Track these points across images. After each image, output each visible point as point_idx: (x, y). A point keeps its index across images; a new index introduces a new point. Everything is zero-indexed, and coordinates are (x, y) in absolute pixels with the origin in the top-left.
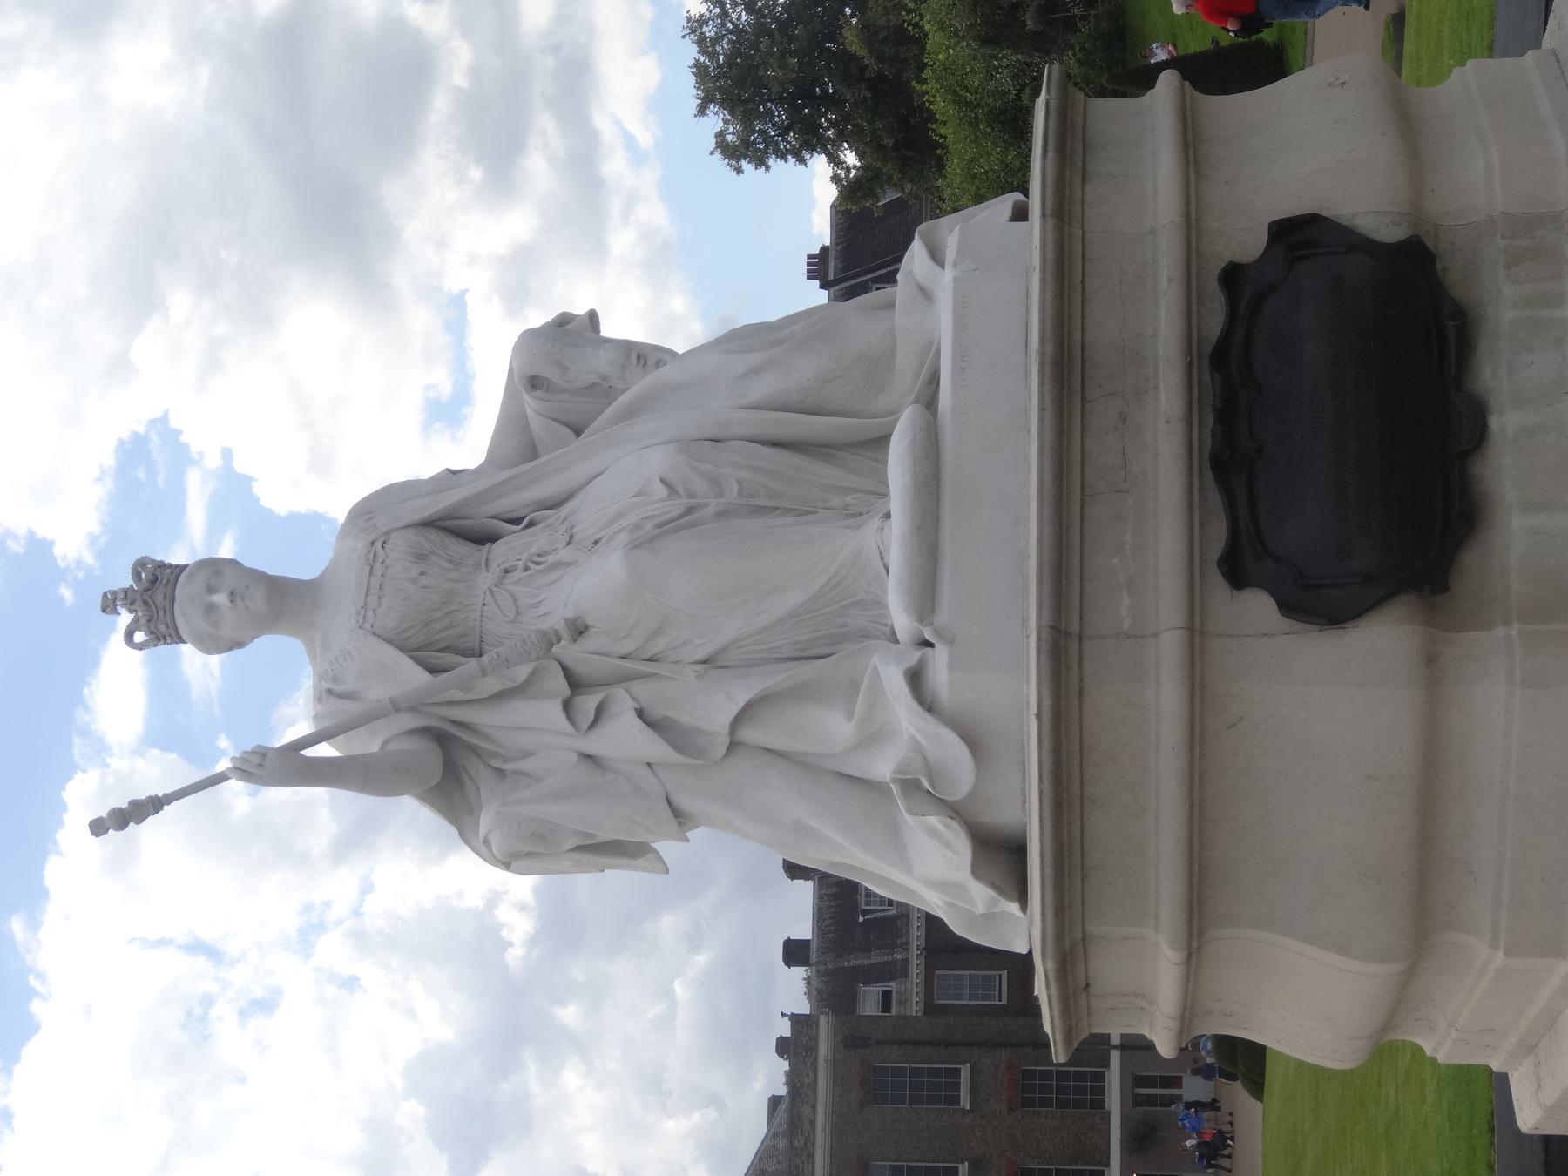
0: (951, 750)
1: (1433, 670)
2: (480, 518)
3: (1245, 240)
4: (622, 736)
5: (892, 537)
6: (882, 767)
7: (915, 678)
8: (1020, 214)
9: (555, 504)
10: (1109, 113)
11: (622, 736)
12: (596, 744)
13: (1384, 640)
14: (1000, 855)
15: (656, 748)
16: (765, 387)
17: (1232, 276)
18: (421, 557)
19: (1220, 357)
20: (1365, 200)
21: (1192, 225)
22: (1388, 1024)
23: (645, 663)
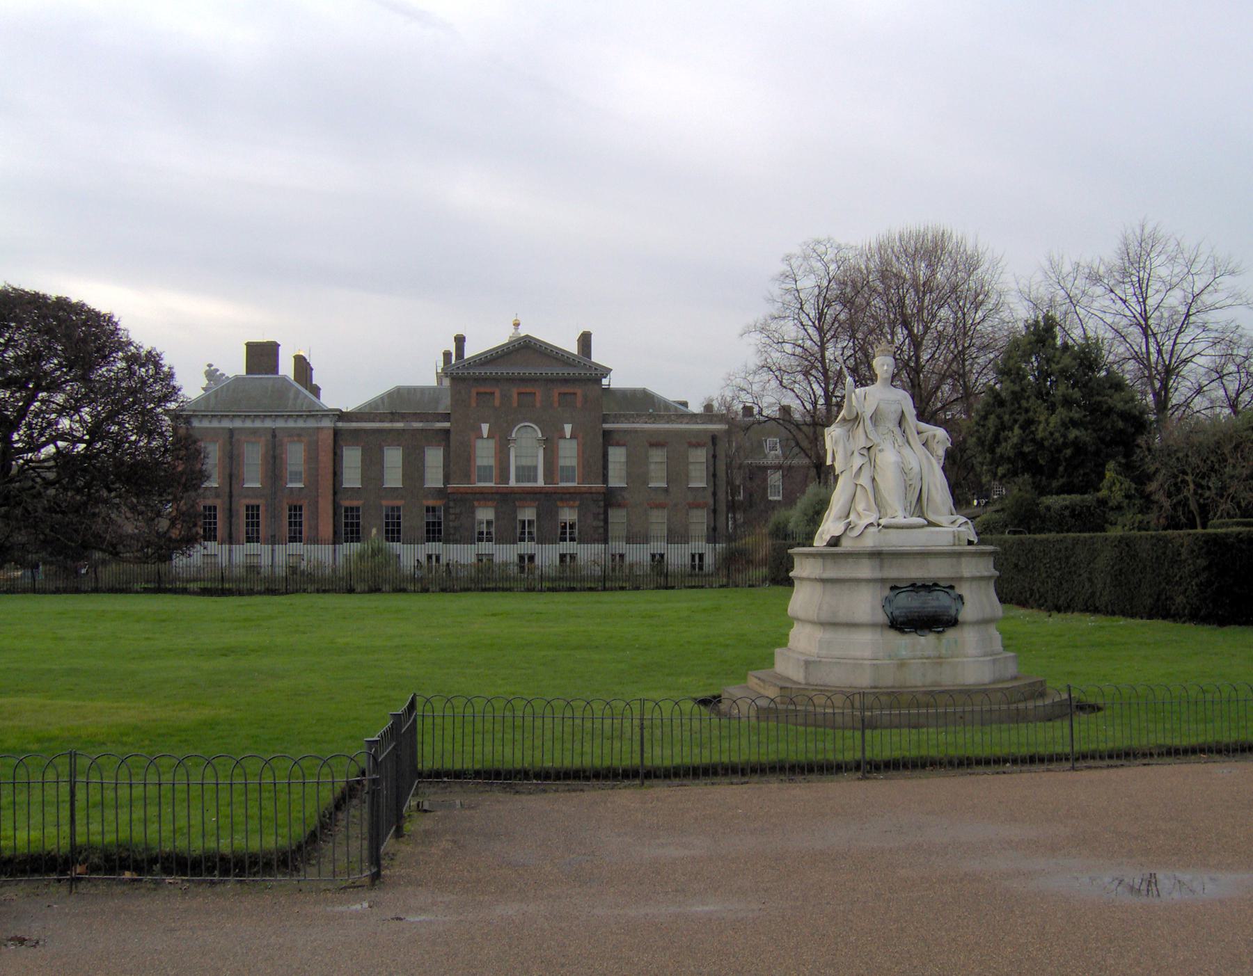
0: (856, 532)
1: (874, 625)
2: (904, 424)
3: (958, 591)
4: (857, 461)
5: (900, 520)
6: (852, 517)
7: (872, 524)
8: (970, 543)
9: (908, 442)
10: (990, 562)
11: (857, 461)
12: (856, 453)
13: (882, 618)
14: (835, 541)
15: (855, 469)
16: (933, 491)
17: (952, 587)
19: (936, 585)
20: (968, 612)
21: (961, 579)
22: (798, 619)
23: (873, 463)
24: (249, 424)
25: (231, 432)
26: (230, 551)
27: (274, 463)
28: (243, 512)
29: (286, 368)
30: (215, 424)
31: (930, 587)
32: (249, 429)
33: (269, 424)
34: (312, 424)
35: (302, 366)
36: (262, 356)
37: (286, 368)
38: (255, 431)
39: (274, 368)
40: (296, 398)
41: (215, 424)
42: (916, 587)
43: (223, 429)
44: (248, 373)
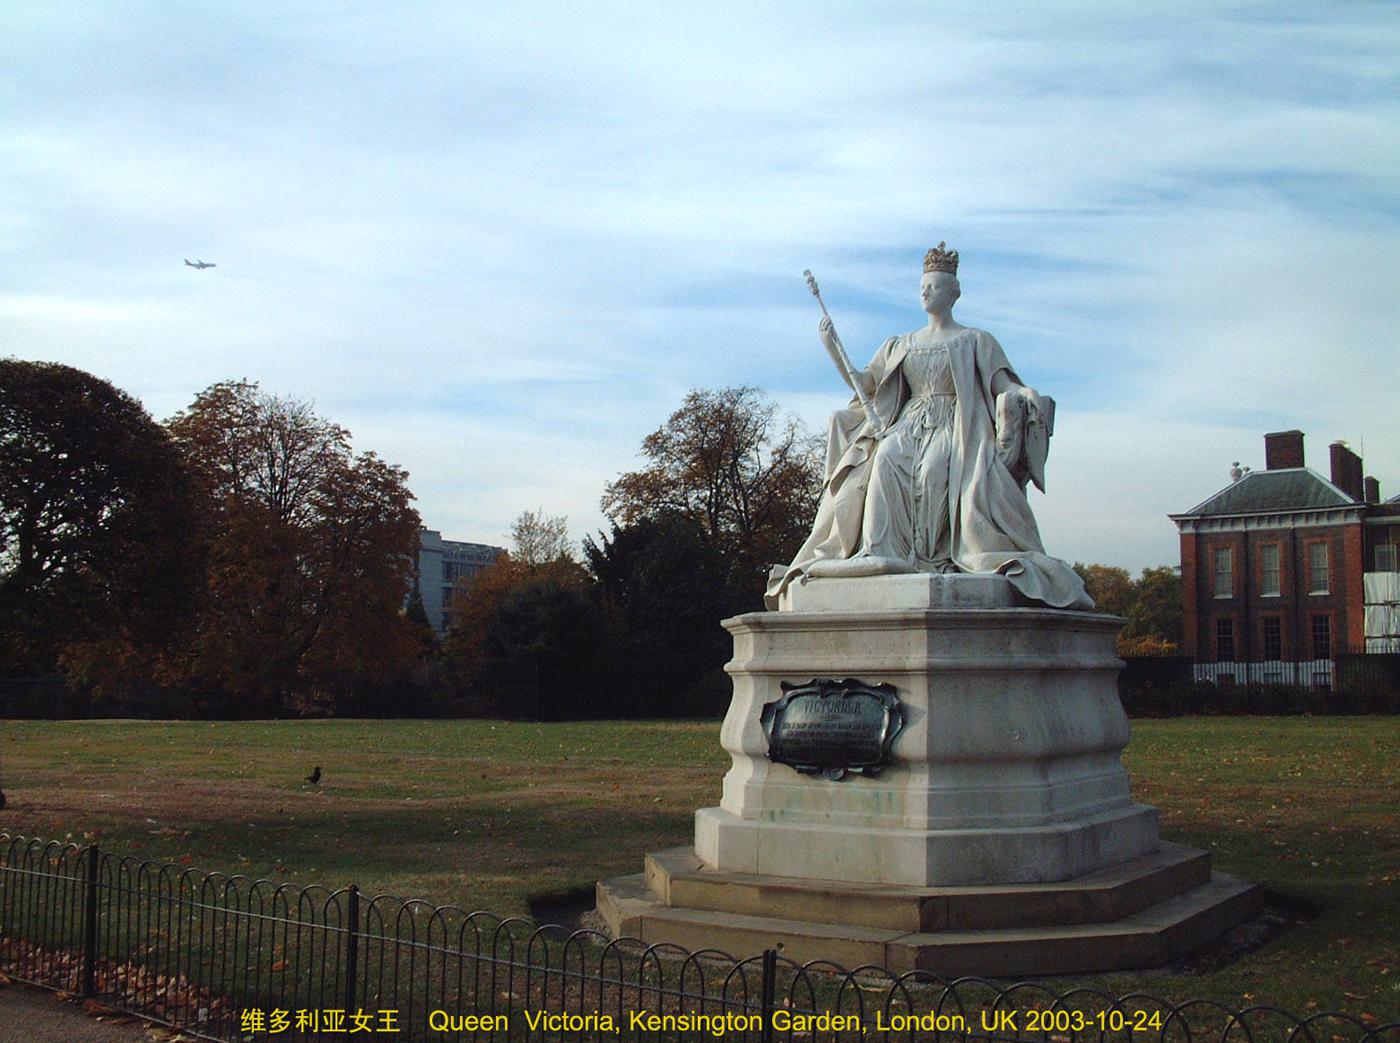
18: (936, 368)
24: (1264, 526)
25: (1246, 534)
26: (1297, 669)
27: (1296, 571)
28: (1260, 624)
29: (1318, 463)
30: (1227, 529)
31: (851, 685)
32: (1264, 531)
33: (1288, 524)
34: (1338, 521)
35: (1345, 462)
36: (1285, 448)
37: (1318, 463)
38: (1271, 534)
39: (1299, 459)
40: (1317, 494)
41: (1227, 529)
42: (824, 686)
43: (1237, 533)
44: (1270, 465)
